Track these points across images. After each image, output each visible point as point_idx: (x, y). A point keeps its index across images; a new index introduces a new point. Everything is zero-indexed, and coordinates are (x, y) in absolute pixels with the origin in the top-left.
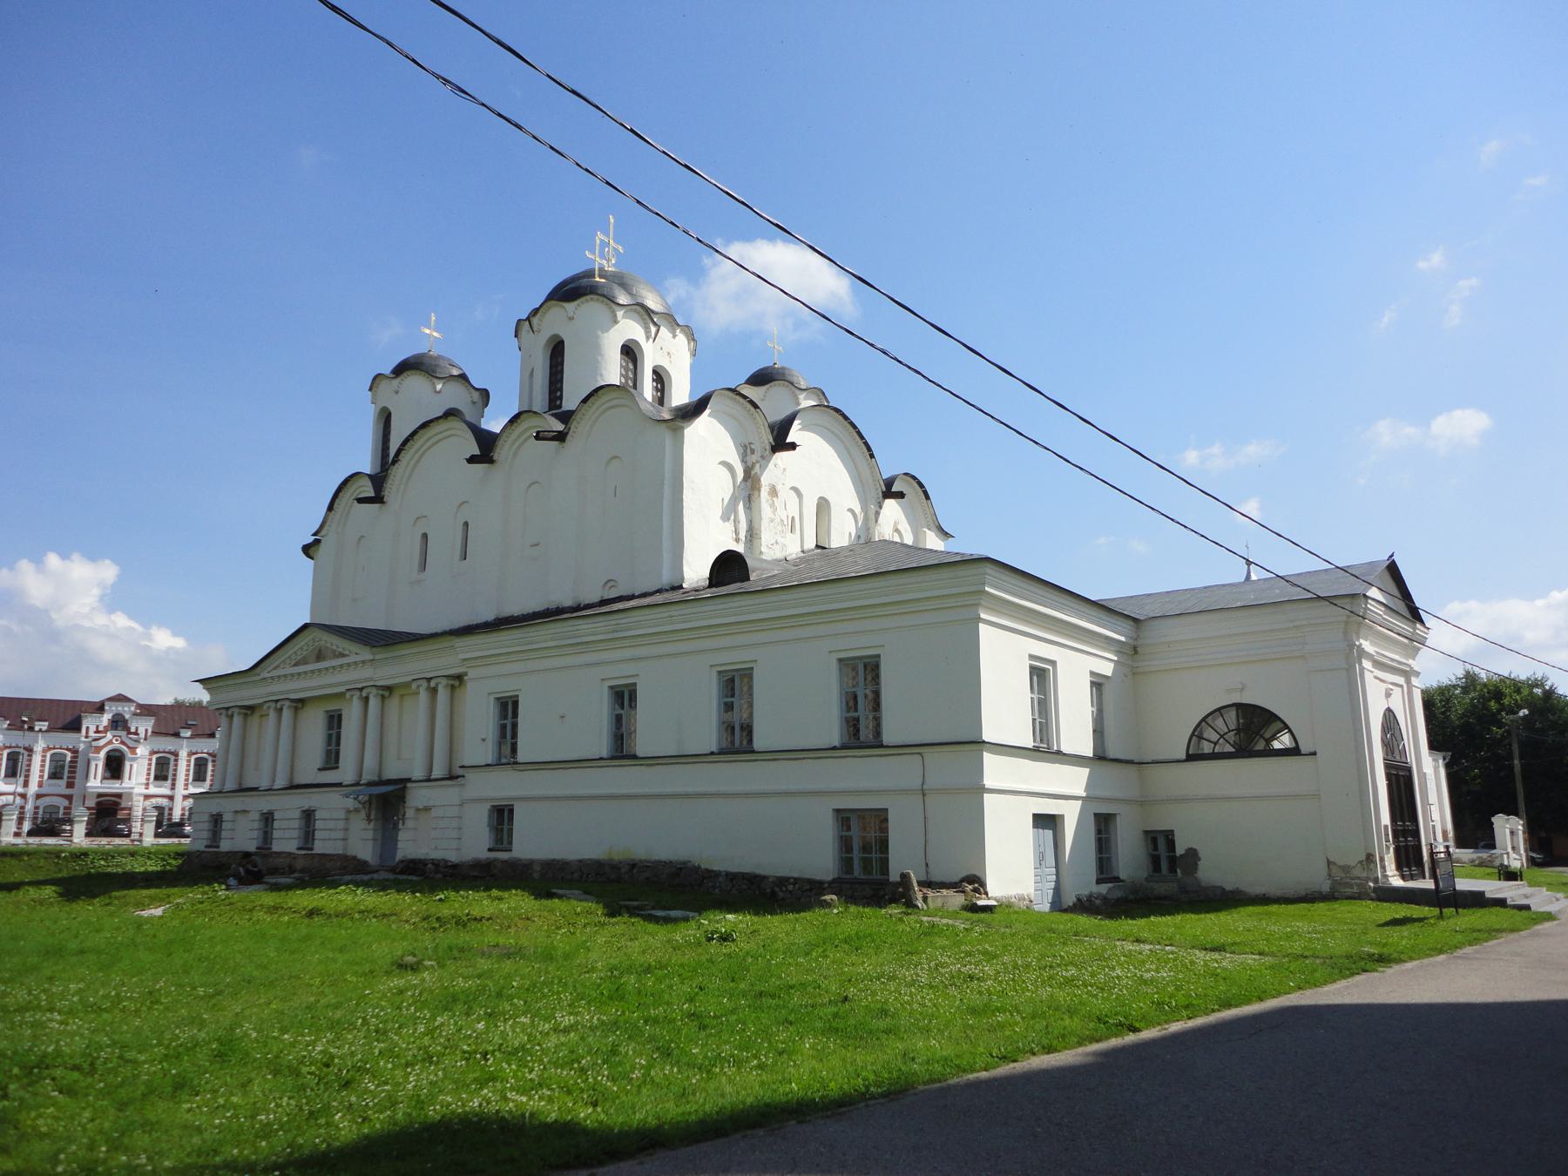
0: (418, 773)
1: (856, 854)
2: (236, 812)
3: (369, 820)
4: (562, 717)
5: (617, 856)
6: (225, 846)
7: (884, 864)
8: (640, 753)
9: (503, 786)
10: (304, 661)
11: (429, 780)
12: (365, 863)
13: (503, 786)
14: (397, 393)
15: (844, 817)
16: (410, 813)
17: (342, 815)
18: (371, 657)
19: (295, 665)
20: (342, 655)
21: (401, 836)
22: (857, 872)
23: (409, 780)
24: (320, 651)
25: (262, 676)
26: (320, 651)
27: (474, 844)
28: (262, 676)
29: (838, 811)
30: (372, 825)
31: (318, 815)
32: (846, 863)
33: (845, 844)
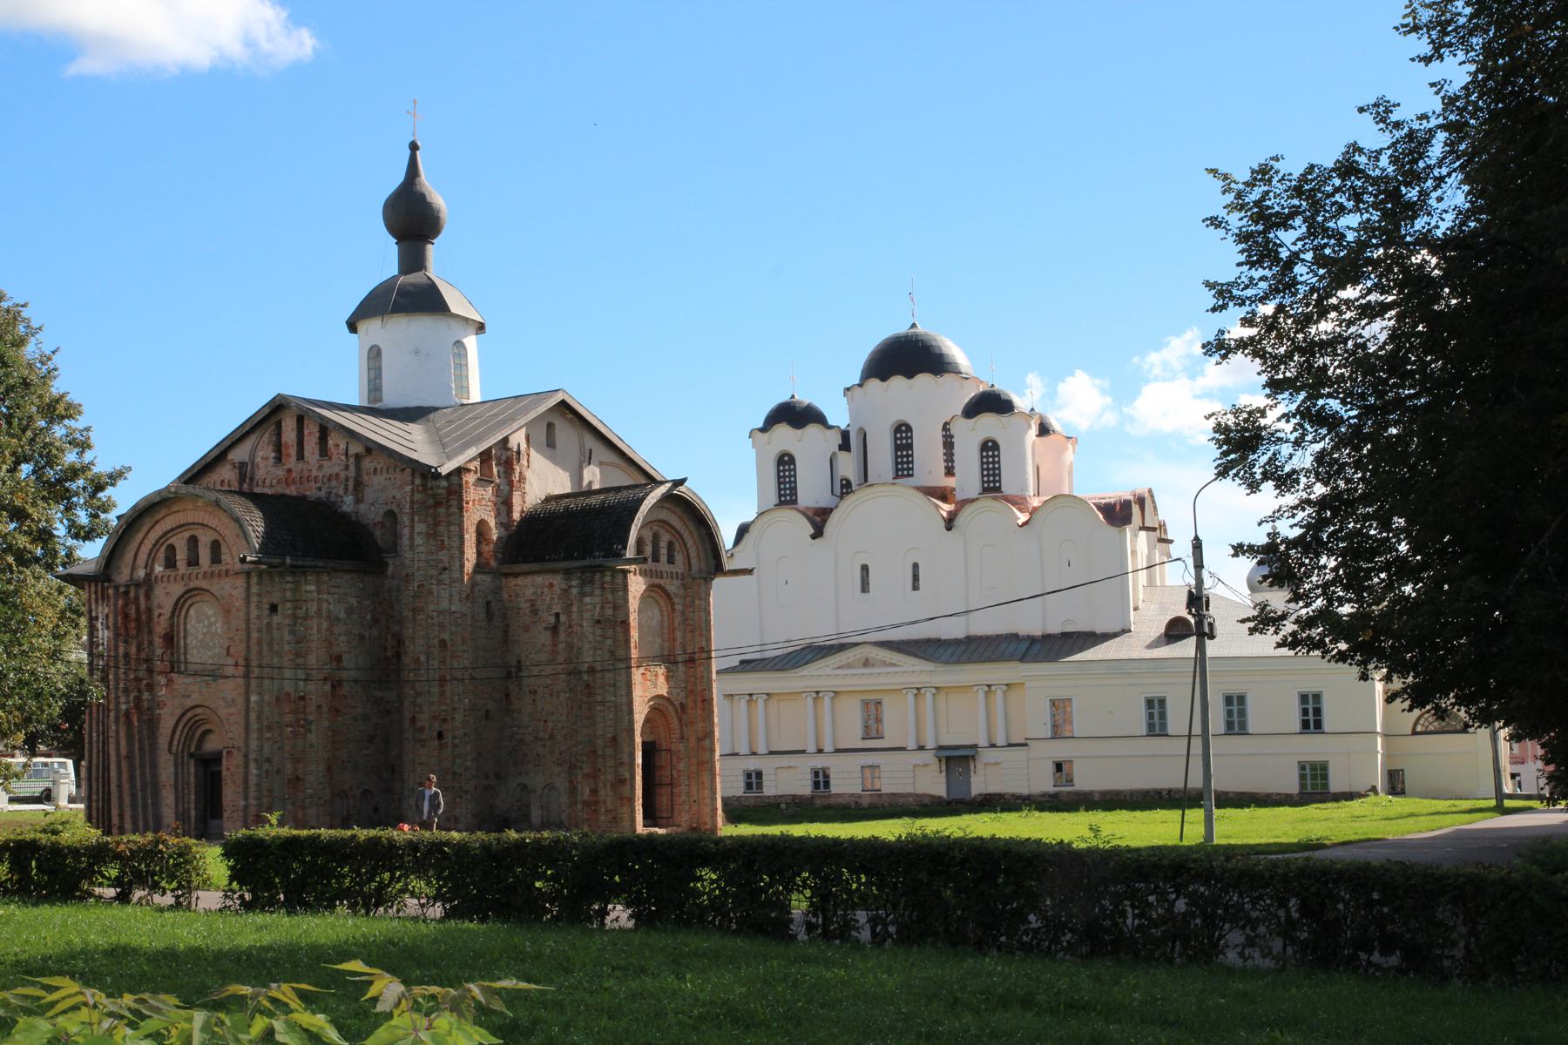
0: (983, 742)
1: (1309, 782)
2: (777, 769)
3: (941, 772)
4: (1111, 712)
5: (1159, 786)
6: (770, 789)
7: (1326, 785)
8: (1170, 733)
9: (1061, 750)
10: (849, 666)
11: (993, 746)
12: (940, 797)
13: (1061, 750)
14: (799, 441)
15: (1303, 768)
16: (980, 766)
17: (911, 768)
18: (932, 669)
19: (839, 668)
20: (894, 665)
21: (972, 779)
22: (1310, 790)
23: (975, 747)
24: (867, 660)
25: (802, 674)
26: (867, 660)
27: (1044, 783)
28: (802, 674)
29: (1299, 762)
30: (944, 774)
31: (882, 767)
32: (1303, 786)
33: (1302, 777)
